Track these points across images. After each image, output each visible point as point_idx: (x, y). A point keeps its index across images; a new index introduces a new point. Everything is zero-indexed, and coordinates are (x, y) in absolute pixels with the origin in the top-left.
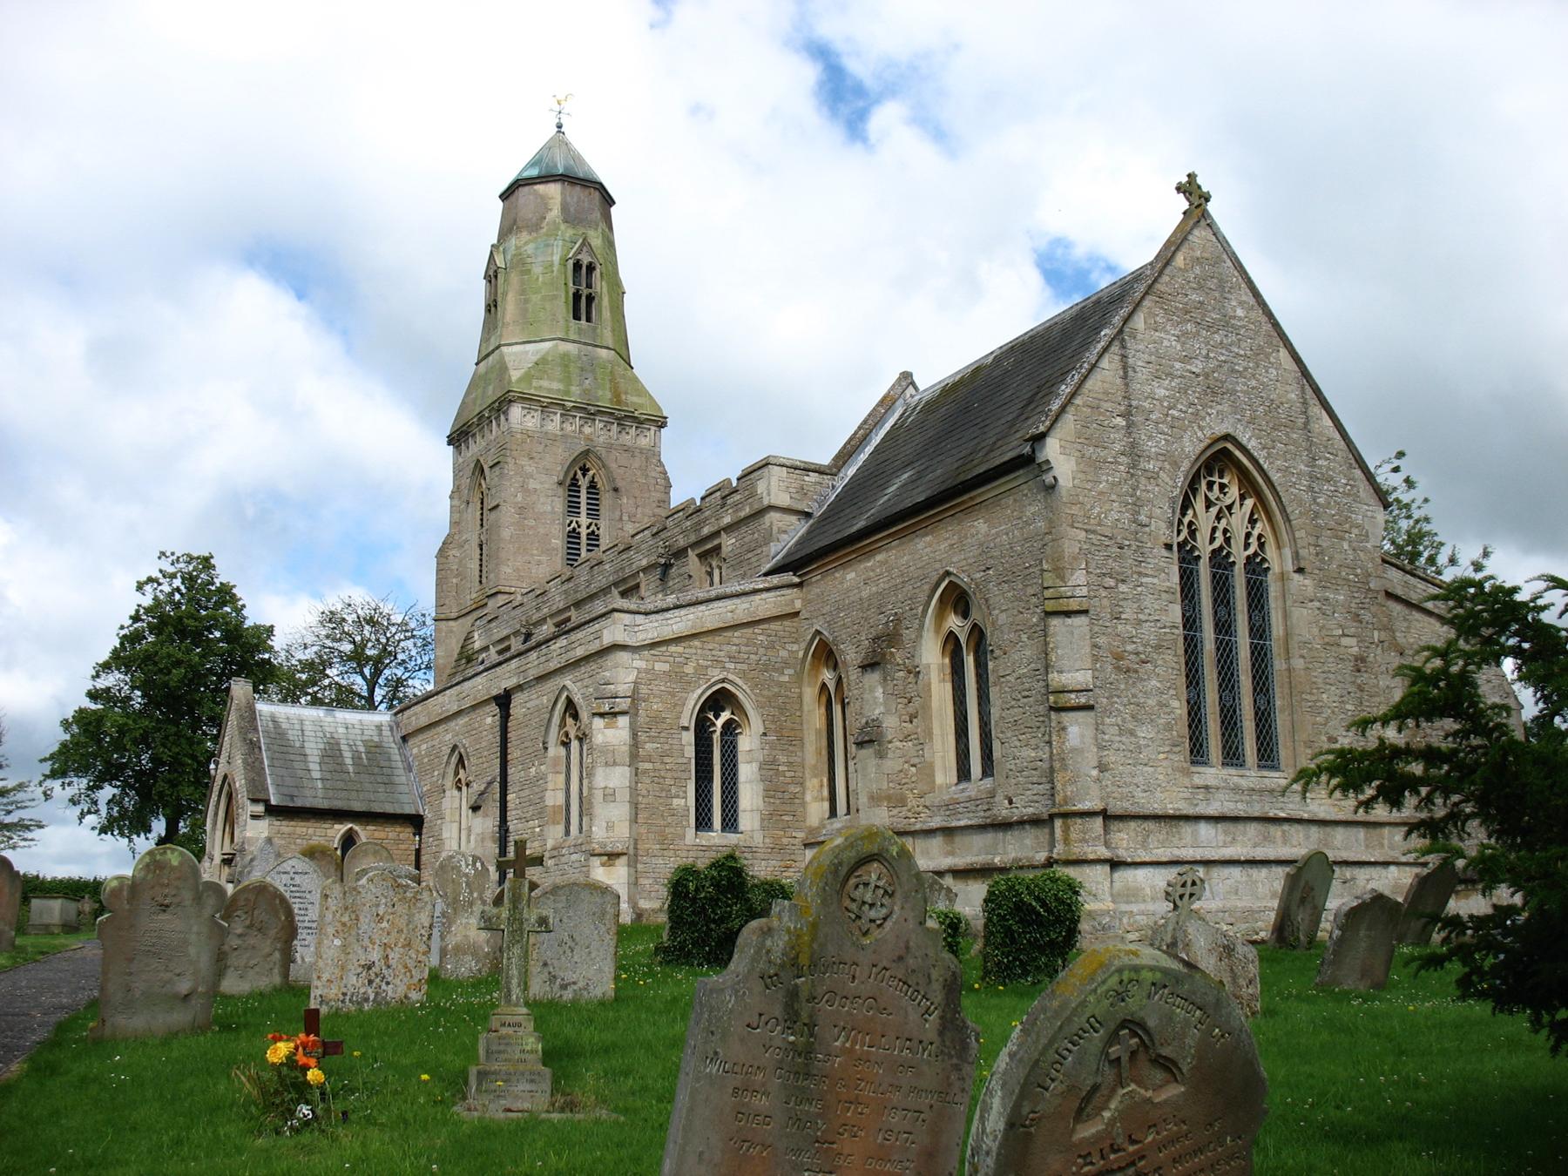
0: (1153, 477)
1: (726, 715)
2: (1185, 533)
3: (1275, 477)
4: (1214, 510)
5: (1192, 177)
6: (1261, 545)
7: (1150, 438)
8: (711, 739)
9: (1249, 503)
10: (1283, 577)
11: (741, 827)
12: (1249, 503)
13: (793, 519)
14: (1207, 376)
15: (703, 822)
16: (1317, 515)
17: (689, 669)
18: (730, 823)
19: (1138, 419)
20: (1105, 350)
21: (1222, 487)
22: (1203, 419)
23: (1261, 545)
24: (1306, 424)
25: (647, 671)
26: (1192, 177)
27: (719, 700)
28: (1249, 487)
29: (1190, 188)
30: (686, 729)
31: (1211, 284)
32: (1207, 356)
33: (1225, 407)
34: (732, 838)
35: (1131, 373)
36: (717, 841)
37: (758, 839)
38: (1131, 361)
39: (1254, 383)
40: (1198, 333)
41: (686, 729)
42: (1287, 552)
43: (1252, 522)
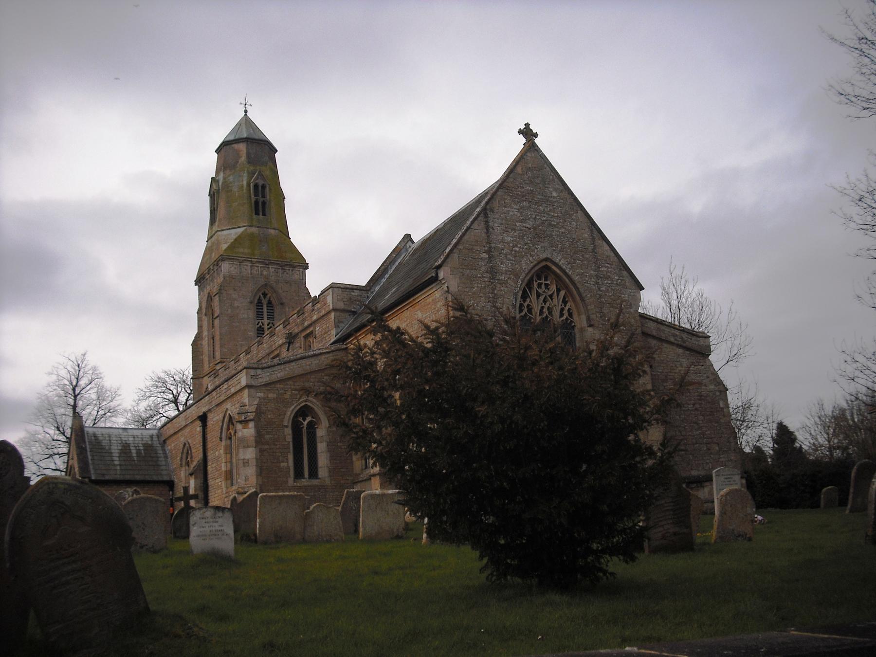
0: (503, 283)
1: (309, 419)
2: (526, 310)
3: (576, 278)
4: (542, 298)
5: (527, 125)
6: (570, 315)
7: (502, 263)
8: (301, 431)
9: (562, 293)
10: (582, 330)
11: (320, 476)
12: (562, 293)
13: (346, 315)
14: (535, 229)
15: (299, 474)
16: (600, 296)
17: (287, 396)
18: (313, 474)
19: (495, 254)
20: (475, 219)
21: (547, 285)
22: (533, 251)
23: (570, 315)
24: (593, 251)
25: (264, 399)
26: (527, 125)
27: (304, 411)
28: (561, 285)
29: (528, 133)
30: (287, 427)
31: (537, 181)
32: (535, 218)
33: (546, 244)
34: (315, 482)
35: (491, 230)
36: (306, 484)
37: (328, 481)
38: (491, 224)
39: (563, 230)
40: (530, 207)
41: (287, 427)
42: (584, 317)
43: (565, 302)
